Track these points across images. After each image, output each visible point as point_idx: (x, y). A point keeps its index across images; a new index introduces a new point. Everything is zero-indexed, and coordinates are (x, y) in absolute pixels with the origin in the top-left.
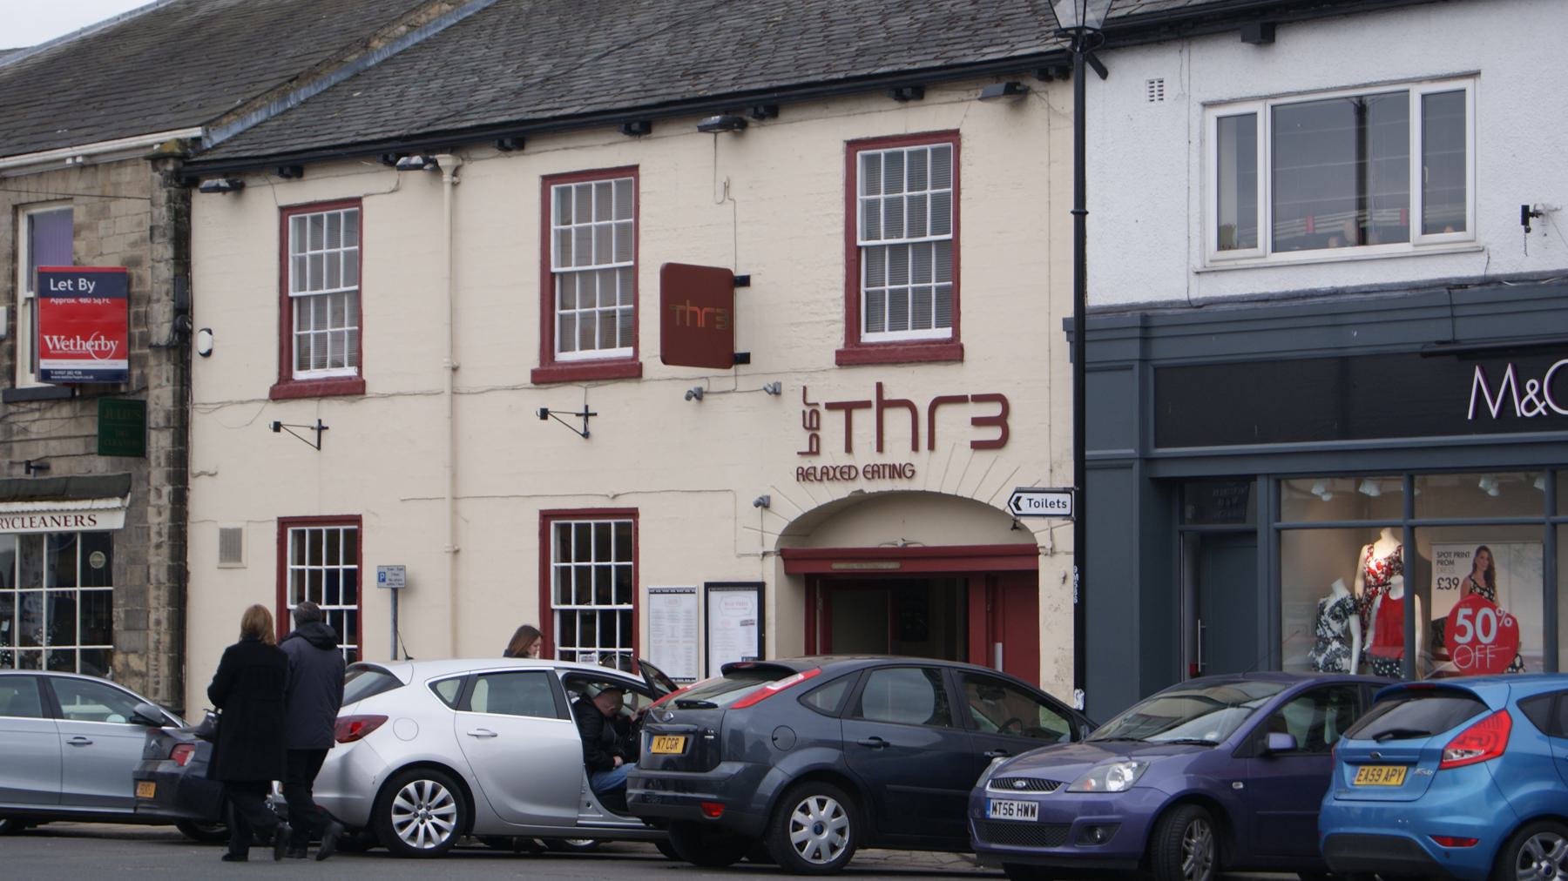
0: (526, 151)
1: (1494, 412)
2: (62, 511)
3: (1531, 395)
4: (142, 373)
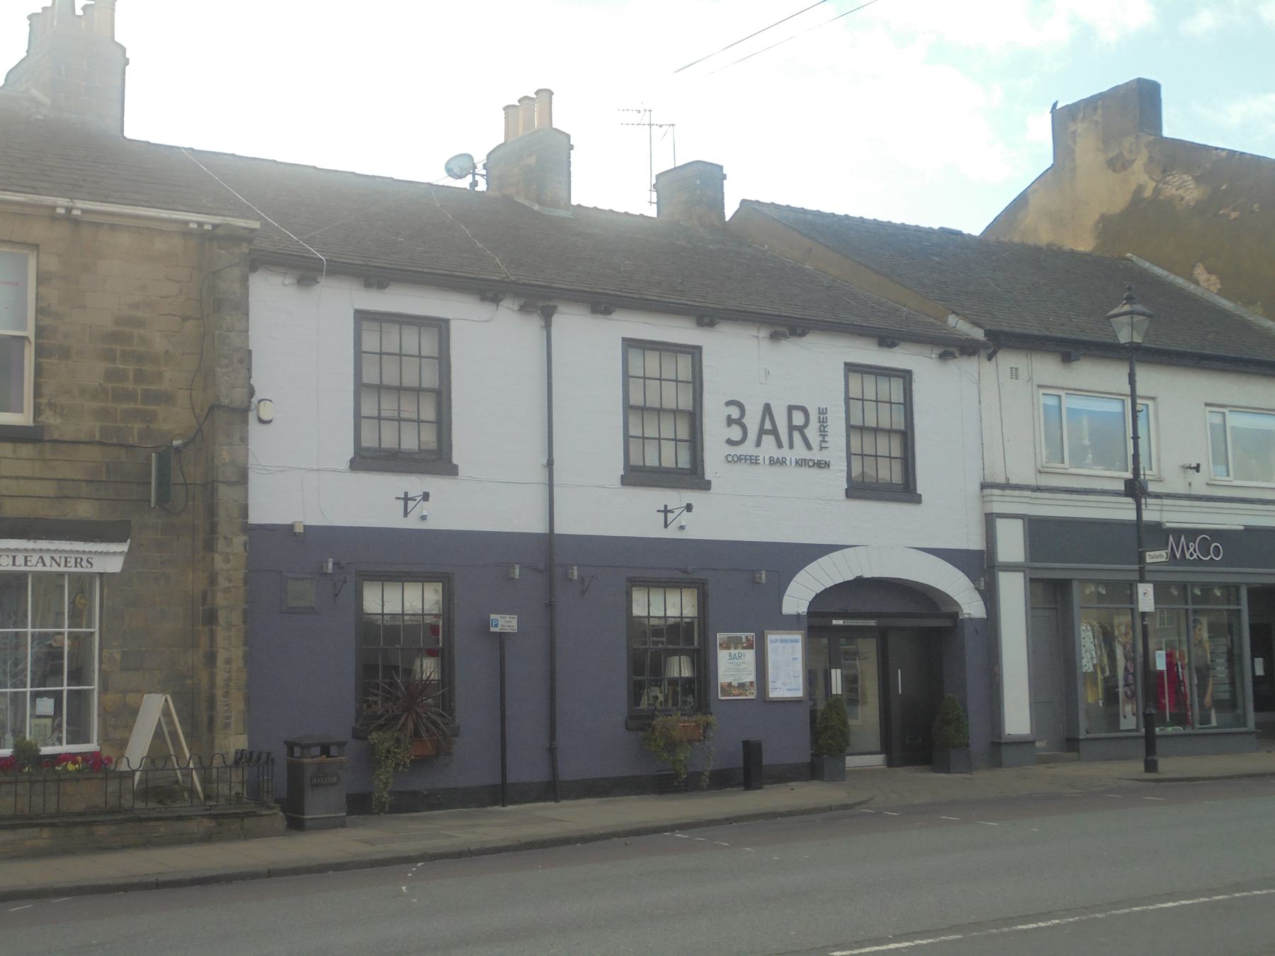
0: (610, 317)
3: (1192, 550)
4: (148, 427)
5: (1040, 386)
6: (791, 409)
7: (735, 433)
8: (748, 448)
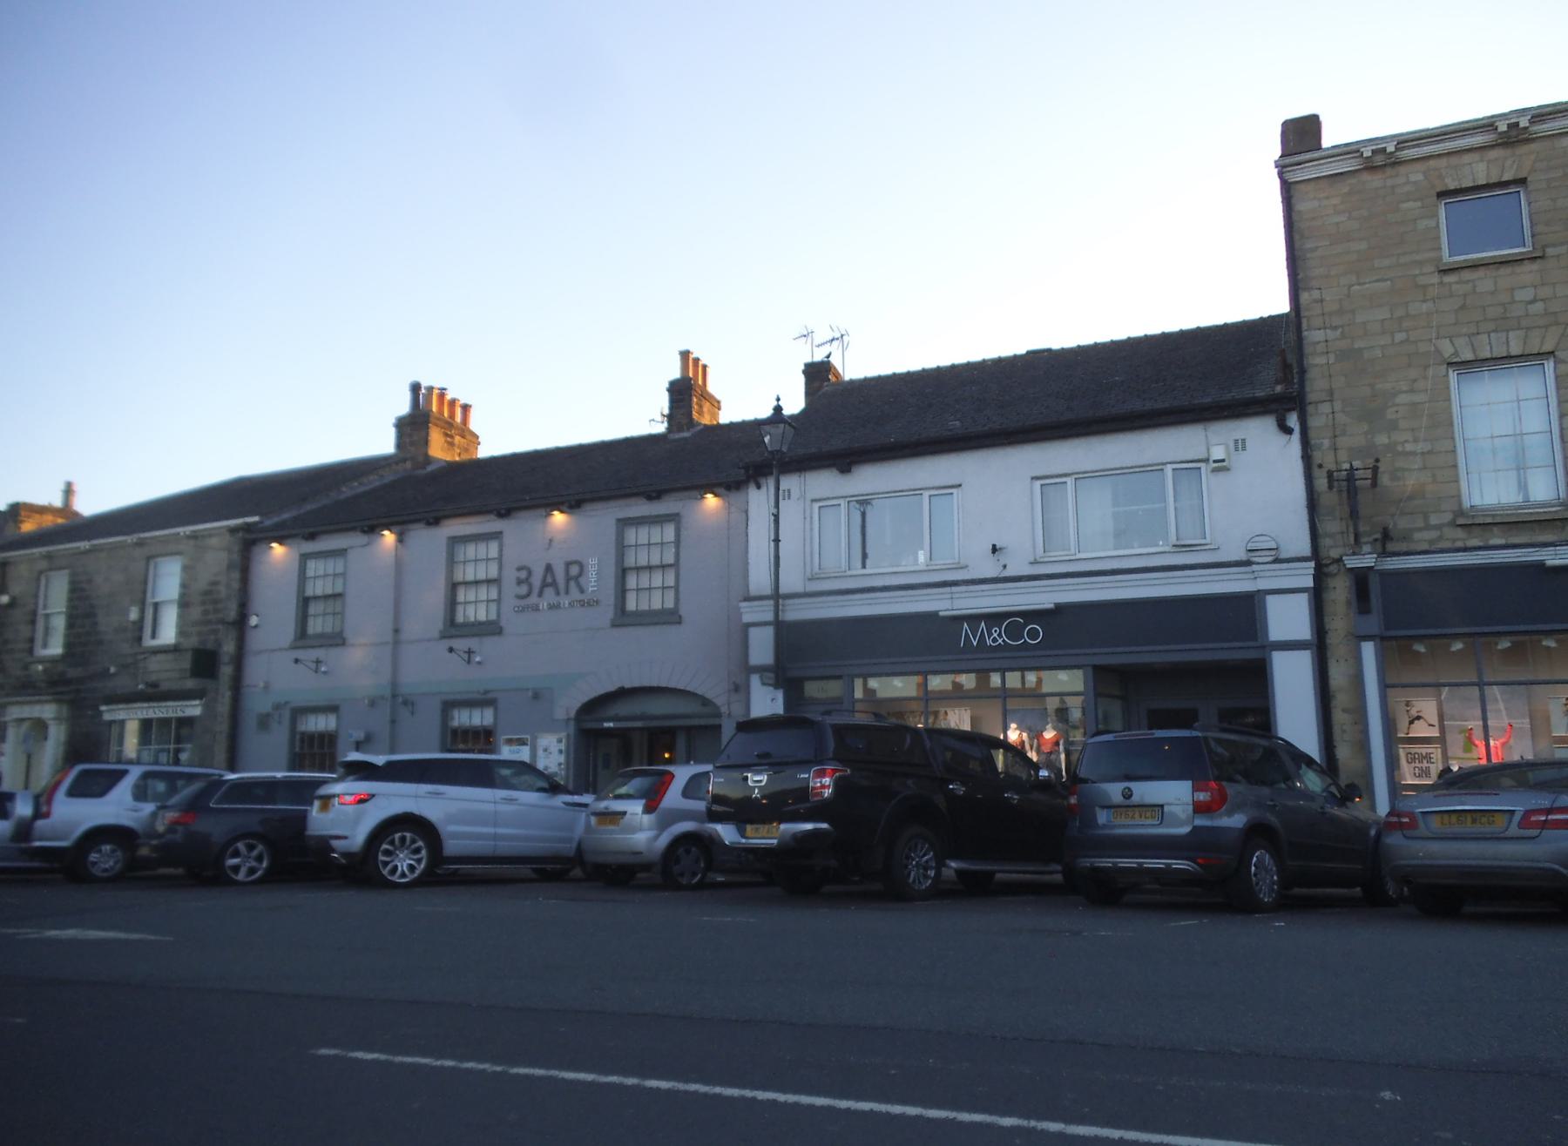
1: (975, 644)
2: (165, 706)
3: (995, 635)
5: (813, 501)
6: (568, 564)
7: (524, 590)
8: (533, 599)
